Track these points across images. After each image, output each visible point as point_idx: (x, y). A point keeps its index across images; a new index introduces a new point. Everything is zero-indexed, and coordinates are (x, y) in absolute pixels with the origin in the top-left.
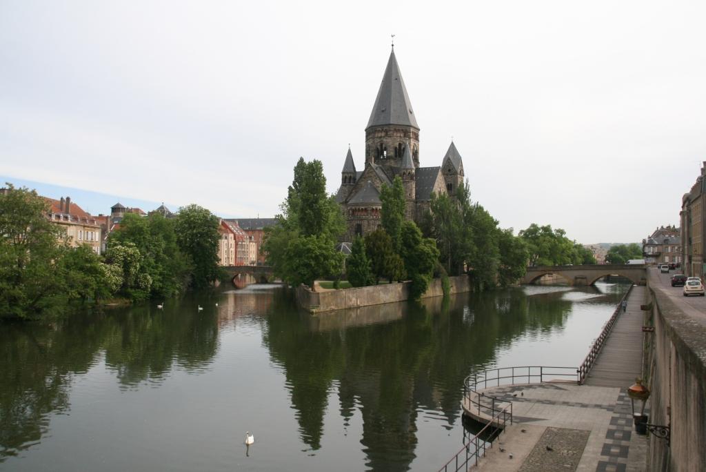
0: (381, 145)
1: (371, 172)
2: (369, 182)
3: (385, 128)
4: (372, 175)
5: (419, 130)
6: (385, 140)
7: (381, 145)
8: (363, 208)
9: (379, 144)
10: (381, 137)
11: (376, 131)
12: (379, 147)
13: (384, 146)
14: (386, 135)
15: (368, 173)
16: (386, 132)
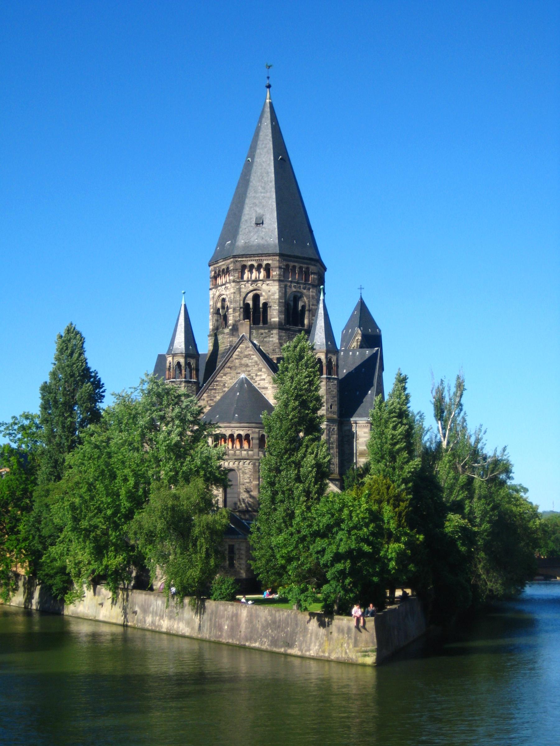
0: (256, 298)
1: (246, 356)
2: (243, 376)
3: (265, 262)
4: (249, 362)
5: (325, 269)
6: (264, 287)
7: (256, 298)
8: (243, 433)
9: (251, 295)
10: (256, 281)
11: (244, 267)
12: (250, 302)
13: (262, 300)
14: (268, 276)
15: (240, 358)
16: (268, 269)
